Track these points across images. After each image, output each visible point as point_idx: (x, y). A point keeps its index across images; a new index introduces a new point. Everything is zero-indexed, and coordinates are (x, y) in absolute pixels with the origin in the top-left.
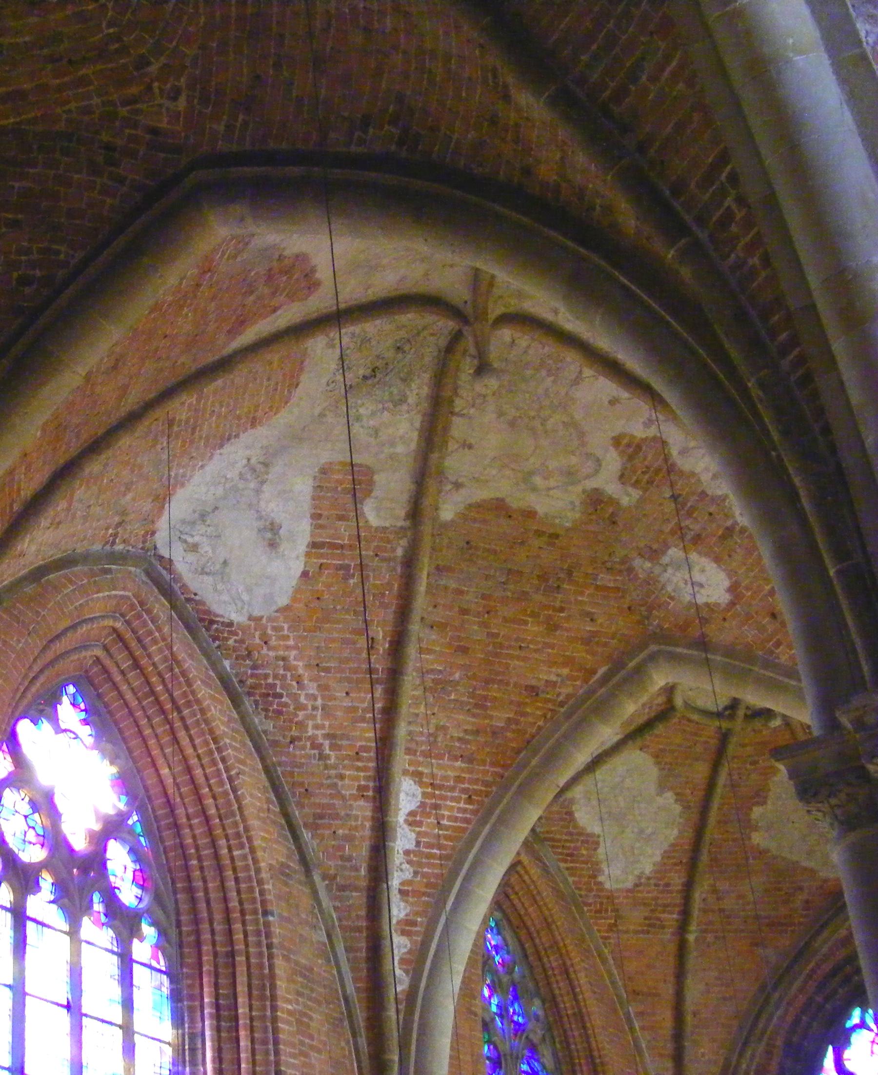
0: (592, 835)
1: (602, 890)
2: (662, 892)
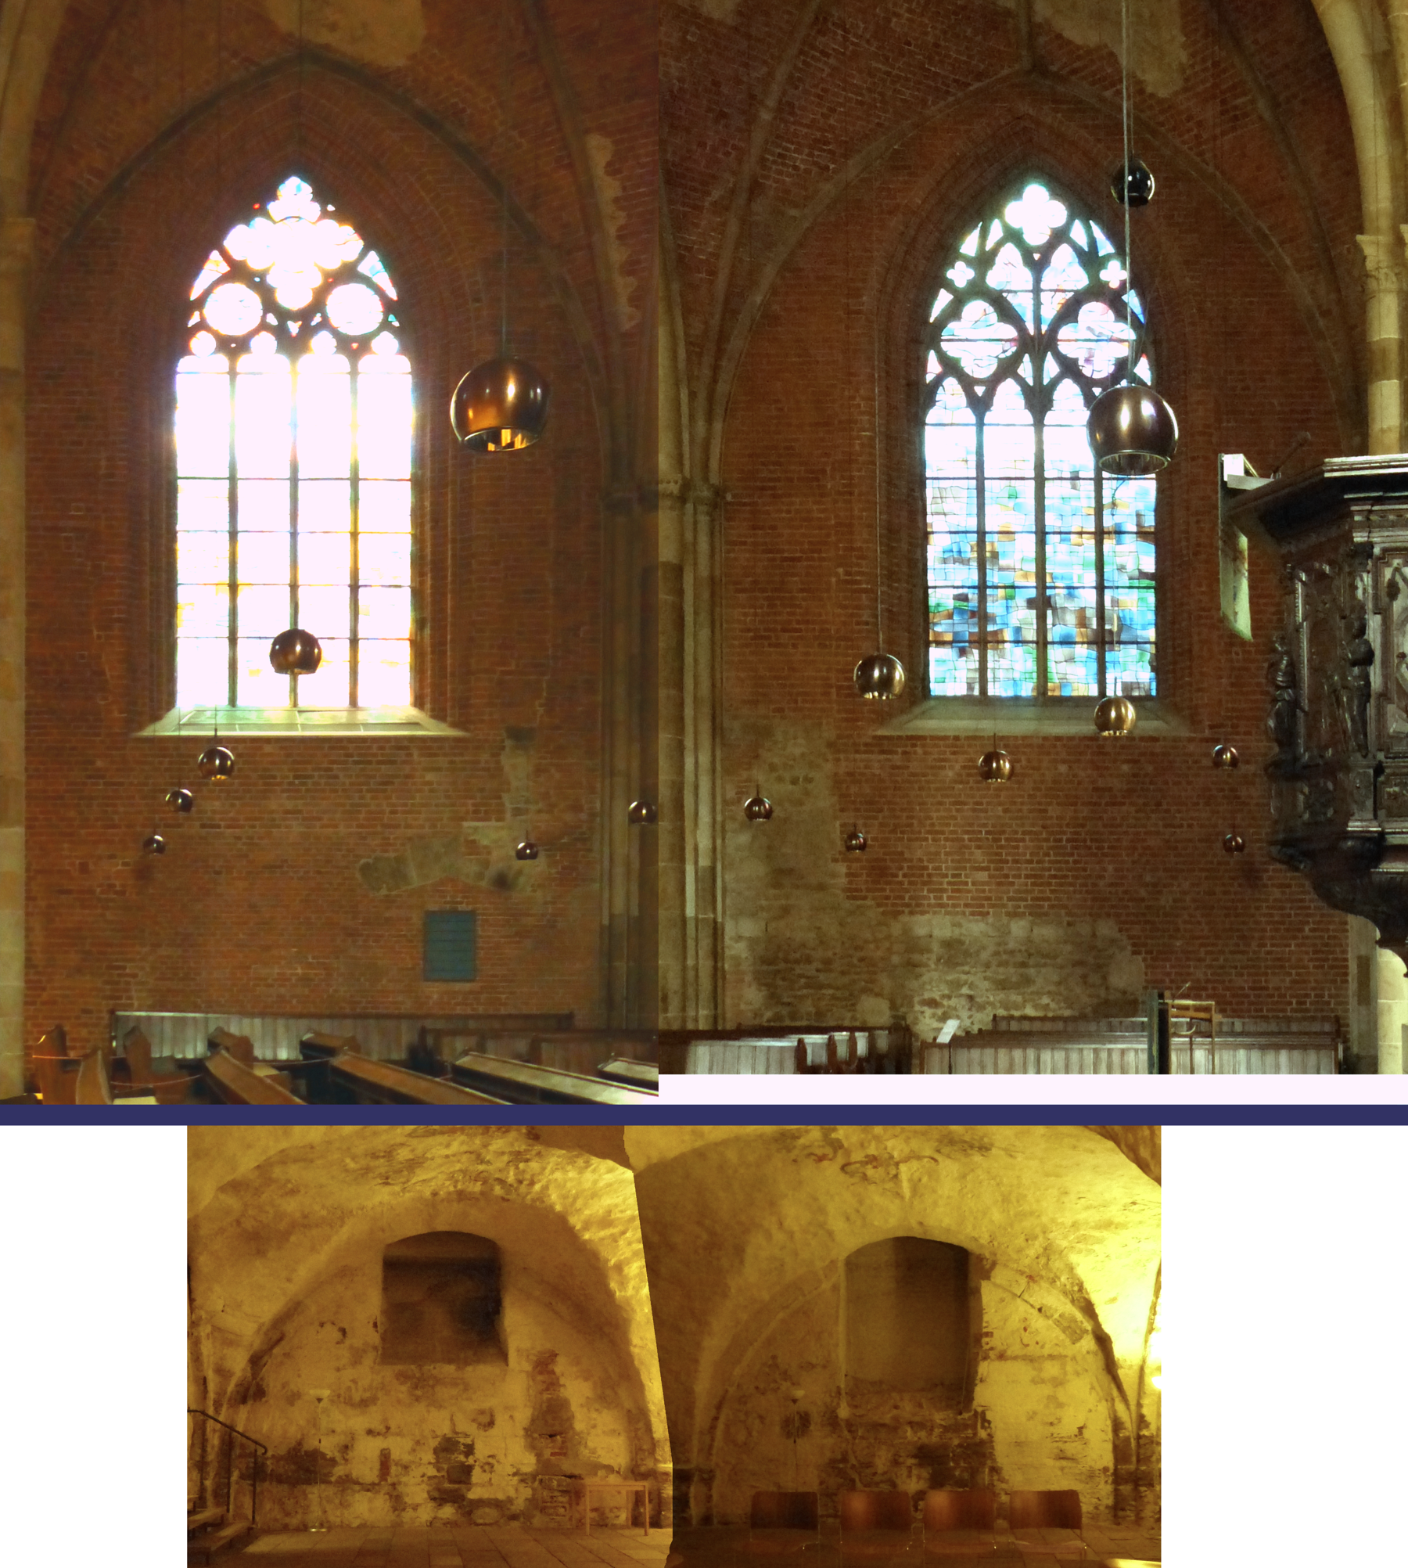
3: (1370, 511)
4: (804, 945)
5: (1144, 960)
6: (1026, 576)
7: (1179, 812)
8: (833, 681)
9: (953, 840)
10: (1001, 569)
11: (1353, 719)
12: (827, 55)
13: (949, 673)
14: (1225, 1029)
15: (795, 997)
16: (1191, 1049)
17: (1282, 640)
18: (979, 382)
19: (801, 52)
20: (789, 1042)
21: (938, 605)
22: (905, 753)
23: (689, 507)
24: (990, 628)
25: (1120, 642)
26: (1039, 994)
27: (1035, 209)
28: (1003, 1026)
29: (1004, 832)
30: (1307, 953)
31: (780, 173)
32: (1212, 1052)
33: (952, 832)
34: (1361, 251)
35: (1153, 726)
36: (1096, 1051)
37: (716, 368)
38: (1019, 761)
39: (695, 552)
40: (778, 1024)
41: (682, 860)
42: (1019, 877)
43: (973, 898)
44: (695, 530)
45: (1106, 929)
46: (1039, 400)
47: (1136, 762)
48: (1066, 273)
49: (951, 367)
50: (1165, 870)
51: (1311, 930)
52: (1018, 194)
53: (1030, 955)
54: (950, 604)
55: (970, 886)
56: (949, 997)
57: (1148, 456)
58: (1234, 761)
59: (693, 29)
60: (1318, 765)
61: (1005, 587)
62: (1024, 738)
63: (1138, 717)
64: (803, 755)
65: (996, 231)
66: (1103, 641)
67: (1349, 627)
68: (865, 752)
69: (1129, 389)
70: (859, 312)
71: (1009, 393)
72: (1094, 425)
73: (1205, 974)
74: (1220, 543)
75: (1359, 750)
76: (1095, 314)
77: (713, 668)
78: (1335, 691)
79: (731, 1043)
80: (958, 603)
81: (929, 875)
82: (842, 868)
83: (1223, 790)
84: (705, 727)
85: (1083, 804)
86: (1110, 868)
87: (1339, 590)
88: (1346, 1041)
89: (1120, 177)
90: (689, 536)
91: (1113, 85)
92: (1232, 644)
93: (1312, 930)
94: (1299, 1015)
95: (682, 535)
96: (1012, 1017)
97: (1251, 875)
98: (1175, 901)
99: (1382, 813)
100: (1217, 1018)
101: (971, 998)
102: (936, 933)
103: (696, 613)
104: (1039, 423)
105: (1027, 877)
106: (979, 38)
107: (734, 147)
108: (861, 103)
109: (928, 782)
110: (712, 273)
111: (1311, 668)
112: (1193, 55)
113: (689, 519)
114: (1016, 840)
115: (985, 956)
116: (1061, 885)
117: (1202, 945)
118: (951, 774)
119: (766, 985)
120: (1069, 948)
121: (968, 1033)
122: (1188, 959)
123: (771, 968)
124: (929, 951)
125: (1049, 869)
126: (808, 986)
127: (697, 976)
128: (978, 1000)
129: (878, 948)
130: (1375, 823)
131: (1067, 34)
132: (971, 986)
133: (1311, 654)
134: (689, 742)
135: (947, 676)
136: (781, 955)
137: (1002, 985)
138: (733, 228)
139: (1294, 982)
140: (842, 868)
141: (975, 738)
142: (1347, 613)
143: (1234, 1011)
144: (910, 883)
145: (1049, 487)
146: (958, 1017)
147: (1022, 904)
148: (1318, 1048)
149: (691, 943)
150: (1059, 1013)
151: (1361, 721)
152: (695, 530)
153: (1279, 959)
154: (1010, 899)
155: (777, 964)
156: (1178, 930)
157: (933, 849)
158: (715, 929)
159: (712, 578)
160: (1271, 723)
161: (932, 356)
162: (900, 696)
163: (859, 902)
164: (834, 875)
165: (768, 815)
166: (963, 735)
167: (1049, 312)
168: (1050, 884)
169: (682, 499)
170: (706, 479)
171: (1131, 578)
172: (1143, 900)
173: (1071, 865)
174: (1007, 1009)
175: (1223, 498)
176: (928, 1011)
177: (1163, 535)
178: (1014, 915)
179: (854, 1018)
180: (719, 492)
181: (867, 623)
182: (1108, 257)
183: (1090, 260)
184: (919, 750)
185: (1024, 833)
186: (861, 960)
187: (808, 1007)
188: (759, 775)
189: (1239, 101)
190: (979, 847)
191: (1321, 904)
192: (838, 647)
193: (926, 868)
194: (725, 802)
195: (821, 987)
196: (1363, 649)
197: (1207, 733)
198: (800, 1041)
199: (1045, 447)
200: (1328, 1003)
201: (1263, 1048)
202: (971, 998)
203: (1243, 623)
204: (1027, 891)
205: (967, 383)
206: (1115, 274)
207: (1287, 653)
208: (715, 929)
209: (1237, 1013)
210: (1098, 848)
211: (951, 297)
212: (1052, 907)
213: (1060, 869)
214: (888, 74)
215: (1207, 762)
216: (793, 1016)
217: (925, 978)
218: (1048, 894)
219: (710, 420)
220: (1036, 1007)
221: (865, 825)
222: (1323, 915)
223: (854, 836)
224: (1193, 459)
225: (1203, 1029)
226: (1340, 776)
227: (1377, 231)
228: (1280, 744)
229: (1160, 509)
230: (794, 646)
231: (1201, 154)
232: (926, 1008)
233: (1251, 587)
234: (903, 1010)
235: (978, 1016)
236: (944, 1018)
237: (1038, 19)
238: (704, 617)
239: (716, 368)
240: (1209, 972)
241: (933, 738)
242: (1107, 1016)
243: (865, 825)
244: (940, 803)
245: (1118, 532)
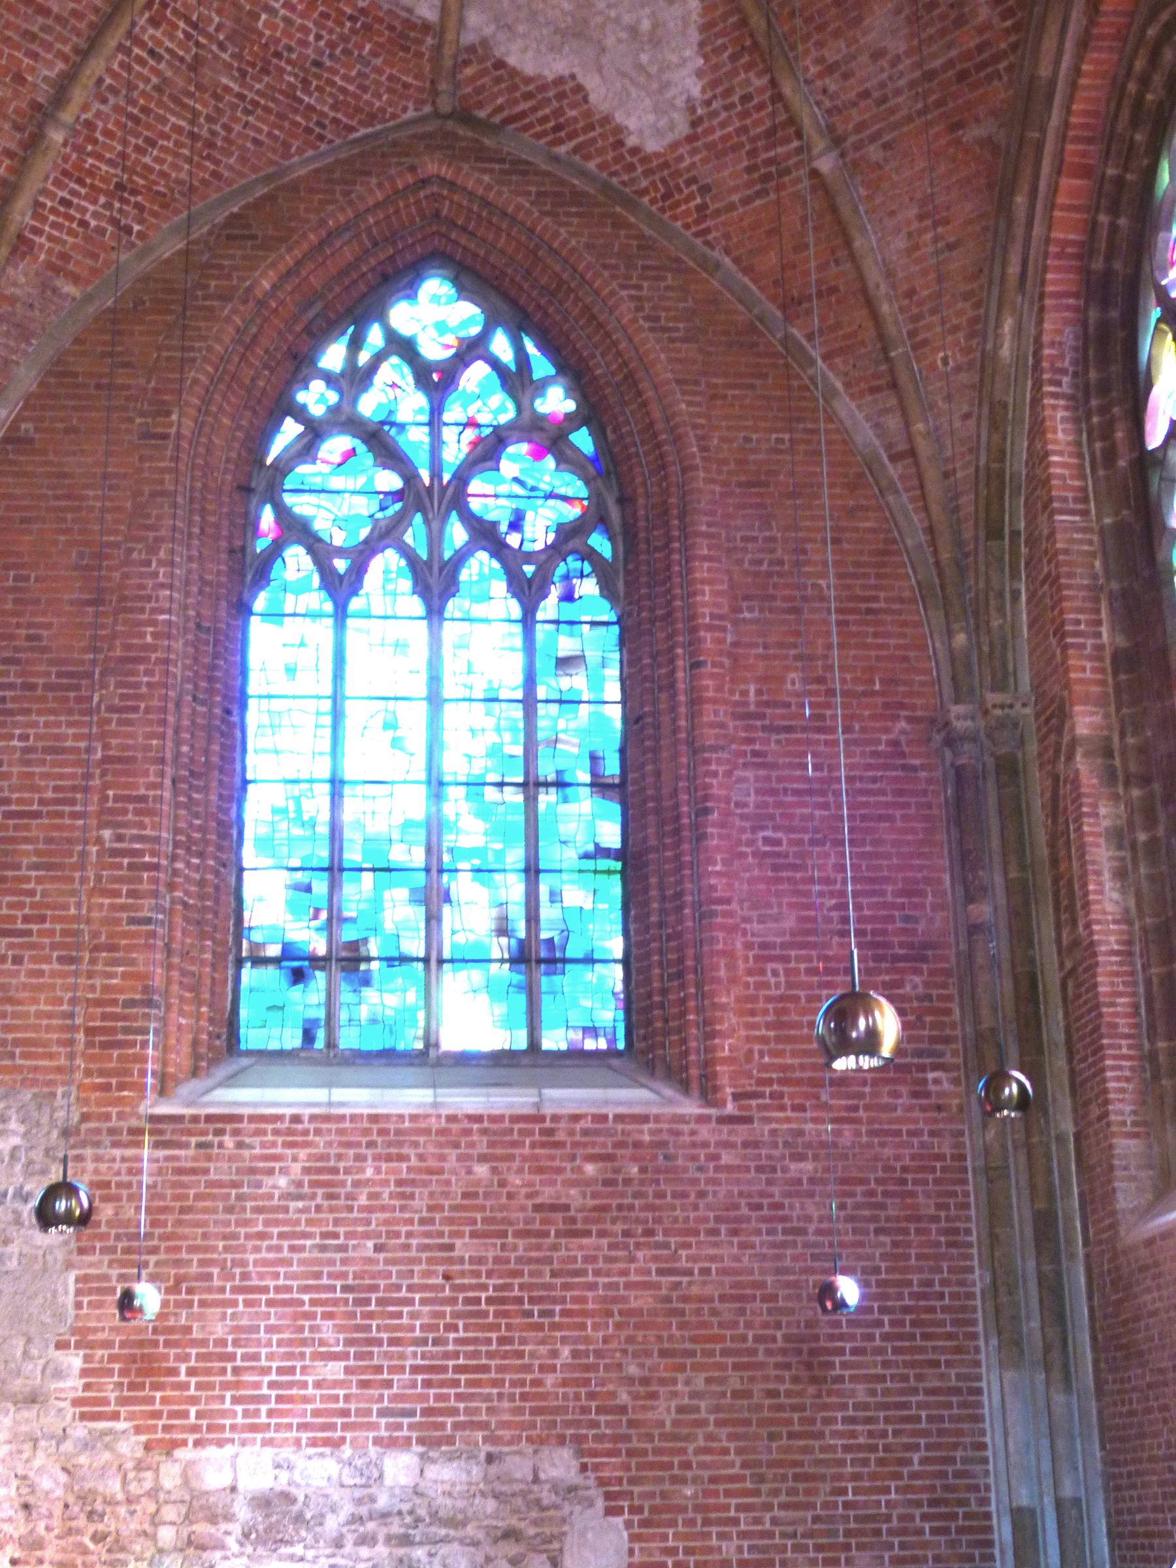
0: (560, 80)
1: (646, 159)
2: (744, 115)
5: (628, 1524)
7: (687, 1246)
8: (78, 1021)
18: (341, 552)
27: (434, 312)
46: (436, 583)
47: (610, 1158)
48: (481, 399)
49: (295, 529)
50: (663, 1353)
62: (414, 1118)
65: (375, 337)
81: (236, 1371)
83: (759, 1207)
85: (519, 1234)
105: (415, 1369)
109: (240, 1197)
115: (332, 1524)
120: (491, 1505)
122: (706, 1522)
124: (229, 1517)
125: (456, 1355)
141: (327, 1118)
145: (450, 712)
154: (382, 1413)
168: (455, 1383)
172: (623, 1410)
178: (391, 1444)
183: (516, 381)
190: (328, 1316)
192: (93, 961)
193: (231, 1357)
197: (730, 1108)
206: (556, 401)
211: (300, 428)
212: (456, 1426)
230: (17, 960)
241: (253, 1118)
244: (262, 1236)
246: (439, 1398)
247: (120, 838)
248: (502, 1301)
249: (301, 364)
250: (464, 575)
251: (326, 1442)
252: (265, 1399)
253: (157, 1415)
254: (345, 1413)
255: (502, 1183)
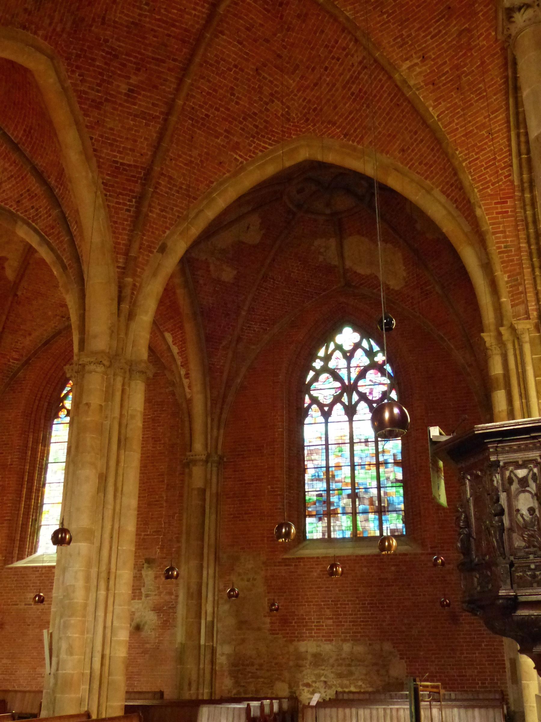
3: (497, 447)
4: (251, 657)
5: (406, 662)
6: (347, 484)
7: (419, 588)
9: (316, 605)
10: (336, 482)
11: (497, 541)
12: (267, 289)
13: (314, 529)
14: (447, 697)
15: (246, 683)
16: (431, 708)
17: (461, 506)
19: (257, 289)
20: (243, 705)
21: (310, 499)
22: (296, 565)
23: (209, 464)
24: (332, 508)
25: (388, 511)
26: (357, 680)
27: (348, 337)
28: (340, 697)
29: (339, 601)
30: (484, 657)
31: (248, 333)
32: (441, 710)
33: (317, 601)
34: (483, 339)
35: (405, 548)
36: (384, 709)
37: (222, 409)
38: (345, 567)
39: (211, 483)
40: (238, 696)
41: (200, 618)
42: (347, 622)
43: (326, 633)
44: (211, 473)
45: (387, 646)
46: (351, 411)
47: (398, 565)
48: (361, 359)
49: (315, 401)
51: (486, 645)
52: (340, 332)
53: (352, 660)
54: (315, 498)
55: (324, 627)
56: (315, 682)
57: (397, 430)
58: (443, 563)
59: (218, 286)
60: (482, 564)
61: (338, 490)
62: (348, 556)
63: (398, 544)
64: (252, 568)
65: (332, 346)
66: (381, 511)
67: (491, 499)
68: (279, 566)
69: (388, 403)
70: (278, 382)
71: (338, 409)
72: (373, 419)
73: (435, 669)
74: (431, 465)
75: (501, 556)
76: (371, 375)
77: (216, 532)
78: (487, 528)
79: (218, 706)
80: (318, 498)
81: (306, 622)
82: (268, 620)
83: (438, 577)
84: (212, 557)
86: (388, 616)
87: (485, 482)
88: (507, 704)
89: (381, 321)
90: (209, 476)
91: (377, 287)
92: (438, 509)
93: (486, 645)
94: (483, 690)
95: (206, 476)
96: (344, 692)
97: (454, 618)
98: (419, 632)
99: (515, 586)
100: (442, 691)
101: (325, 682)
102: (310, 650)
103: (210, 508)
104: (351, 421)
105: (350, 622)
106: (324, 277)
107: (232, 326)
108: (280, 305)
109: (306, 578)
110: (222, 372)
111: (475, 518)
112: (408, 273)
113: (209, 469)
114: (345, 604)
115: (331, 661)
116: (366, 625)
117: (433, 654)
118: (315, 574)
119: (234, 677)
120: (370, 656)
121: (324, 700)
122: (427, 661)
123: (237, 668)
124: (306, 659)
125: (360, 618)
126: (252, 677)
127: (204, 673)
128: (329, 683)
129: (283, 658)
130: (512, 591)
131: (358, 271)
132: (326, 676)
133: (475, 512)
134: (205, 565)
135: (314, 529)
136: (241, 662)
137: (340, 676)
138: (230, 355)
139: (479, 672)
140: (268, 620)
141: (326, 557)
142: (490, 492)
143: (450, 688)
144: (298, 626)
146: (320, 692)
147: (348, 635)
148: (494, 707)
149: (202, 657)
150: (367, 689)
151: (501, 541)
152: (211, 473)
153: (471, 661)
154: (342, 633)
155: (240, 666)
156: (421, 646)
157: (308, 610)
158: (213, 650)
159: (217, 493)
160: (459, 545)
161: (307, 397)
162: (293, 540)
163: (275, 636)
164: (264, 623)
165: (237, 596)
166: (320, 556)
167: (354, 376)
168: (360, 625)
169: (207, 461)
170: (216, 453)
171: (392, 483)
172: (404, 632)
173: (370, 616)
174: (342, 688)
175: (431, 446)
176: (306, 689)
177: (405, 462)
178: (345, 640)
179: (272, 693)
180: (221, 458)
181: (280, 509)
182: (377, 352)
183: (370, 354)
184: (302, 564)
185: (348, 601)
186: (276, 664)
187: (252, 688)
188: (234, 578)
189: (428, 288)
190: (328, 608)
191: (489, 632)
193: (305, 619)
194: (219, 591)
195: (258, 677)
196: (499, 508)
197: (430, 551)
198: (248, 705)
199: (354, 430)
200: (497, 683)
201: (466, 707)
202: (325, 682)
203: (443, 499)
204: (350, 629)
205: (321, 406)
206: (380, 358)
207: (464, 512)
208: (213, 650)
209: (452, 689)
210: (382, 607)
211: (314, 373)
212: (362, 636)
213: (365, 618)
214: (290, 293)
215: (430, 564)
216: (245, 692)
217: (304, 673)
218: (360, 630)
219: (219, 429)
220: (355, 686)
221: (278, 599)
222: (490, 638)
223: (273, 605)
224: (417, 430)
225: (436, 698)
226: (493, 568)
227: (490, 331)
228: (464, 554)
229: (403, 452)
230: (250, 520)
231: (413, 309)
232: (305, 688)
233: (445, 483)
234: (295, 688)
235: (329, 692)
236: (313, 693)
237: (347, 267)
238: (213, 510)
239: (222, 409)
240: (437, 668)
241: (308, 558)
242: (389, 691)
243: (278, 599)
244: (311, 588)
245: (386, 463)
246: (356, 629)
247: (272, 488)
248: (372, 604)
249: (313, 357)
250: (358, 408)
251: (329, 640)
252: (313, 629)
253: (288, 633)
254: (333, 633)
255: (371, 573)
